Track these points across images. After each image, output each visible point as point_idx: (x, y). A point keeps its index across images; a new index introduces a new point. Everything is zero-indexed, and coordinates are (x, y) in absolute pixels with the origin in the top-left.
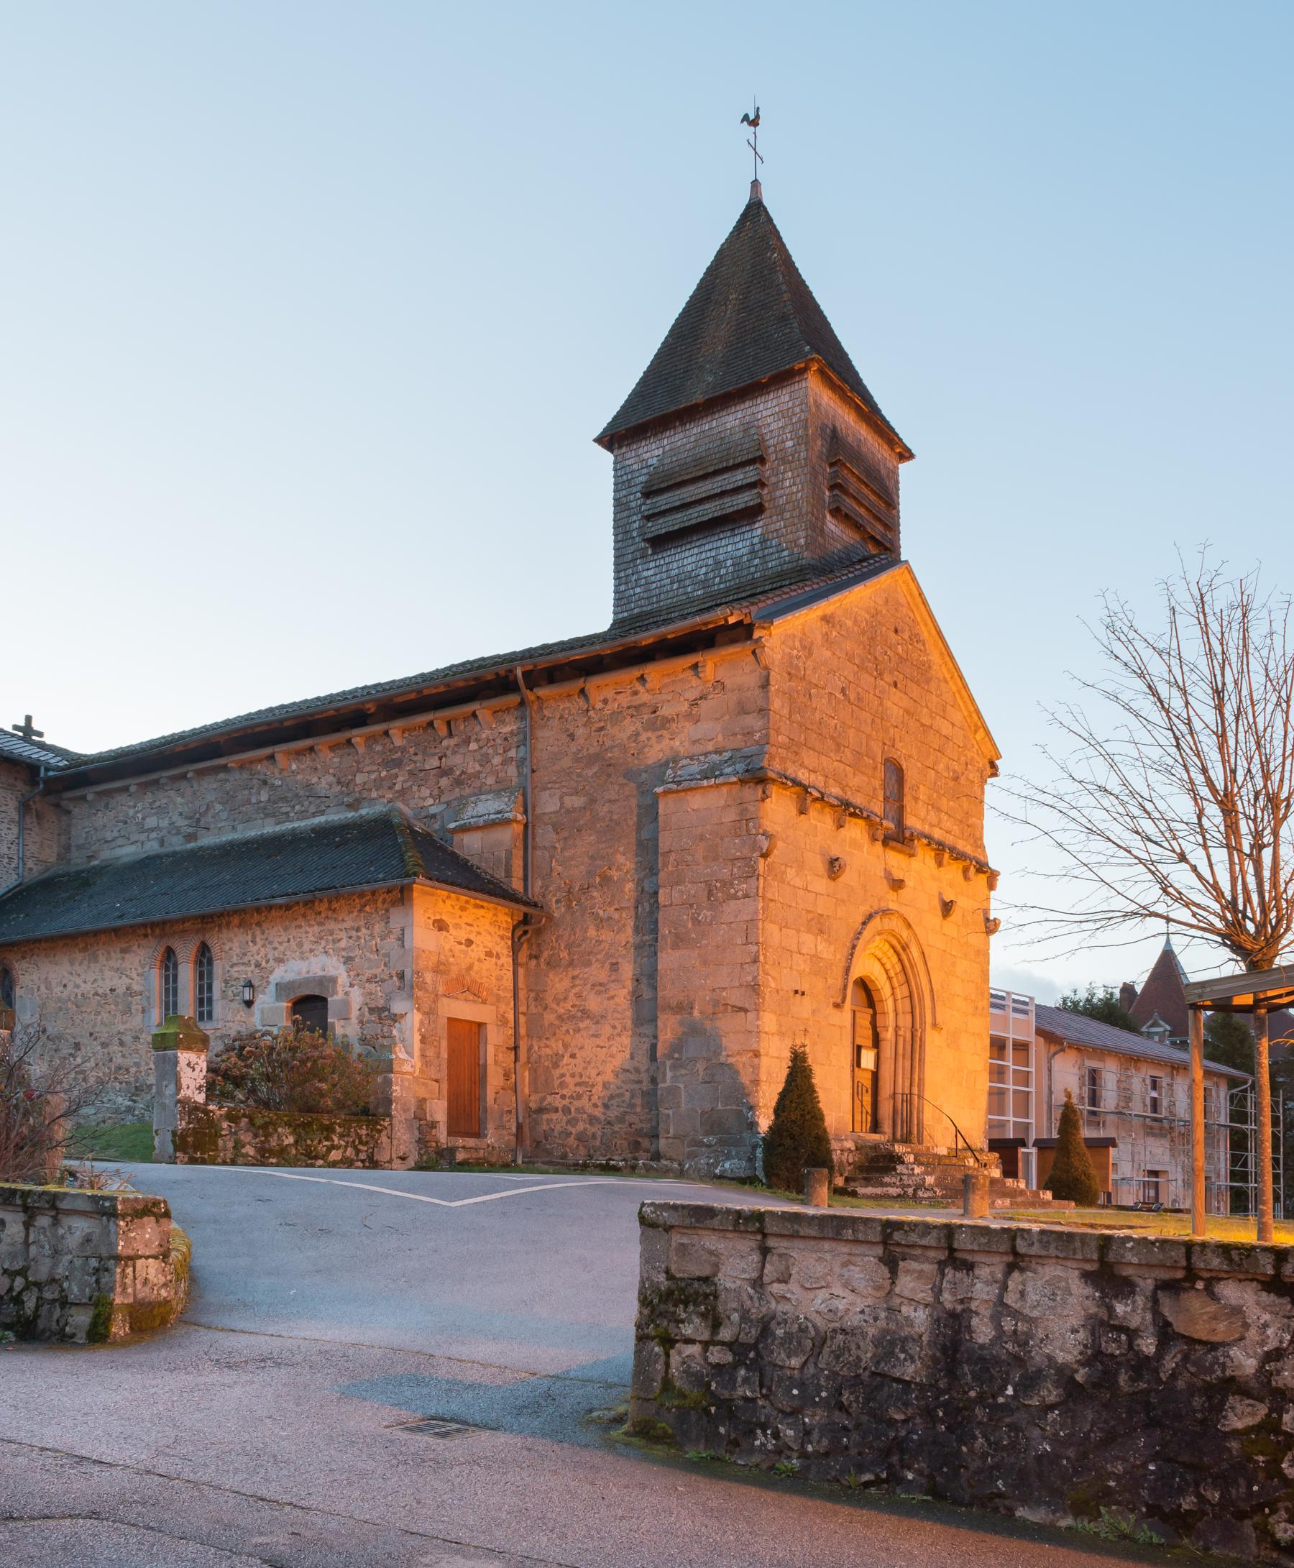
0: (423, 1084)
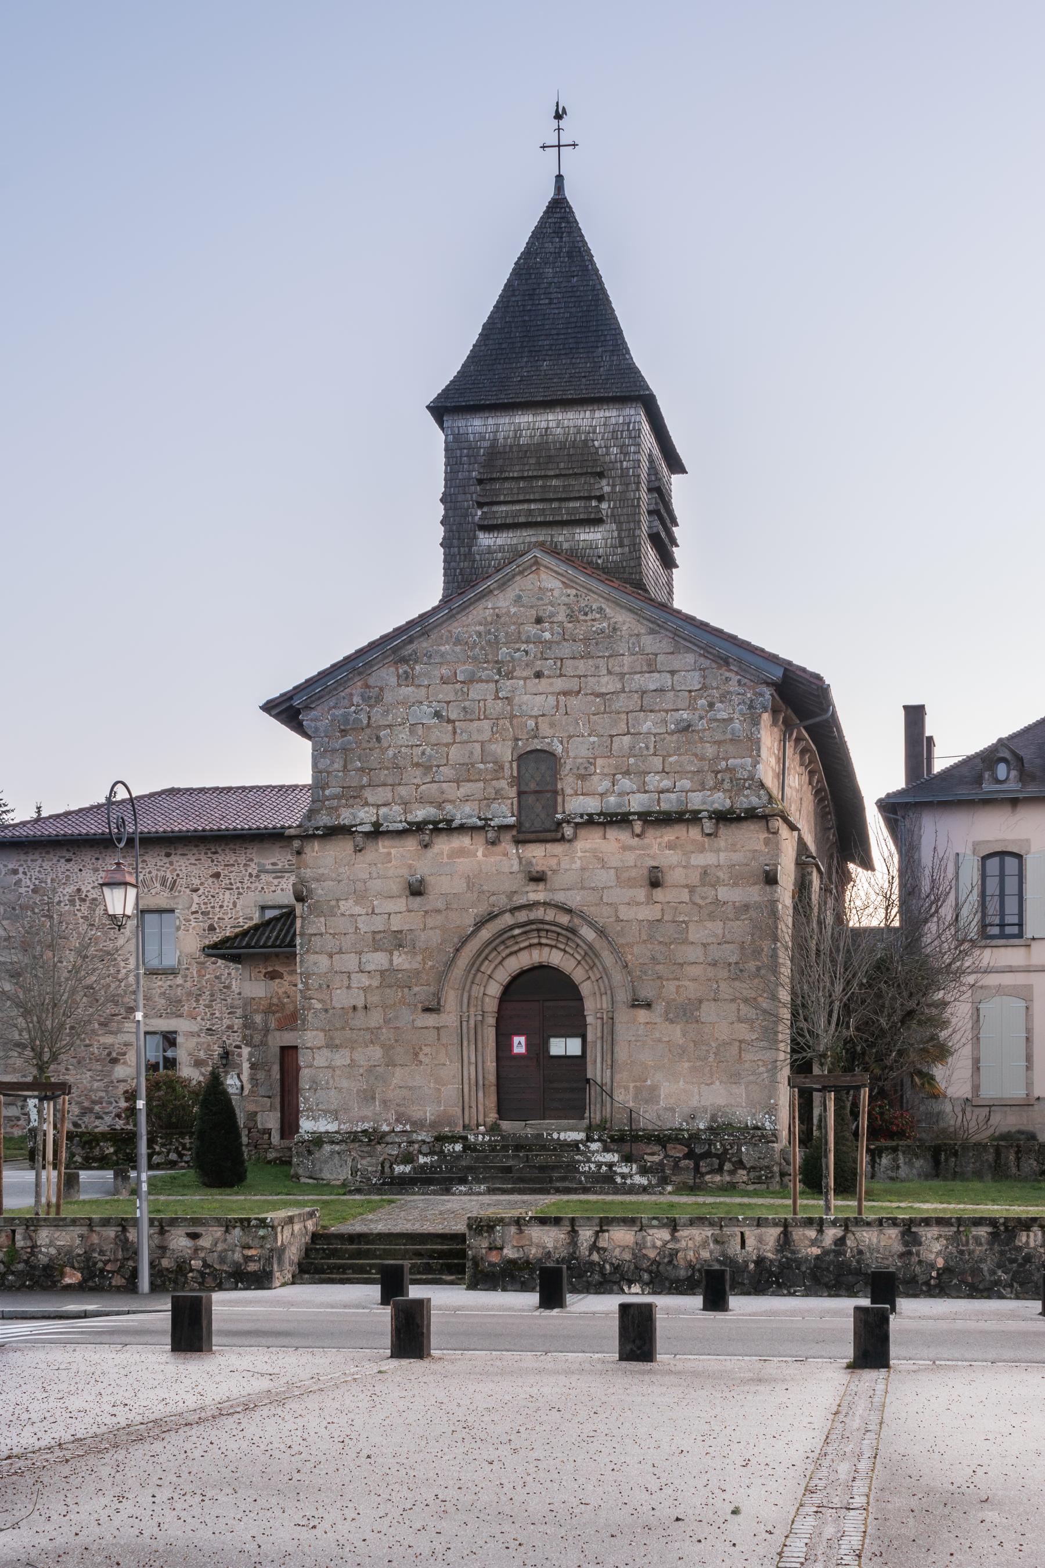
0: (253, 1101)
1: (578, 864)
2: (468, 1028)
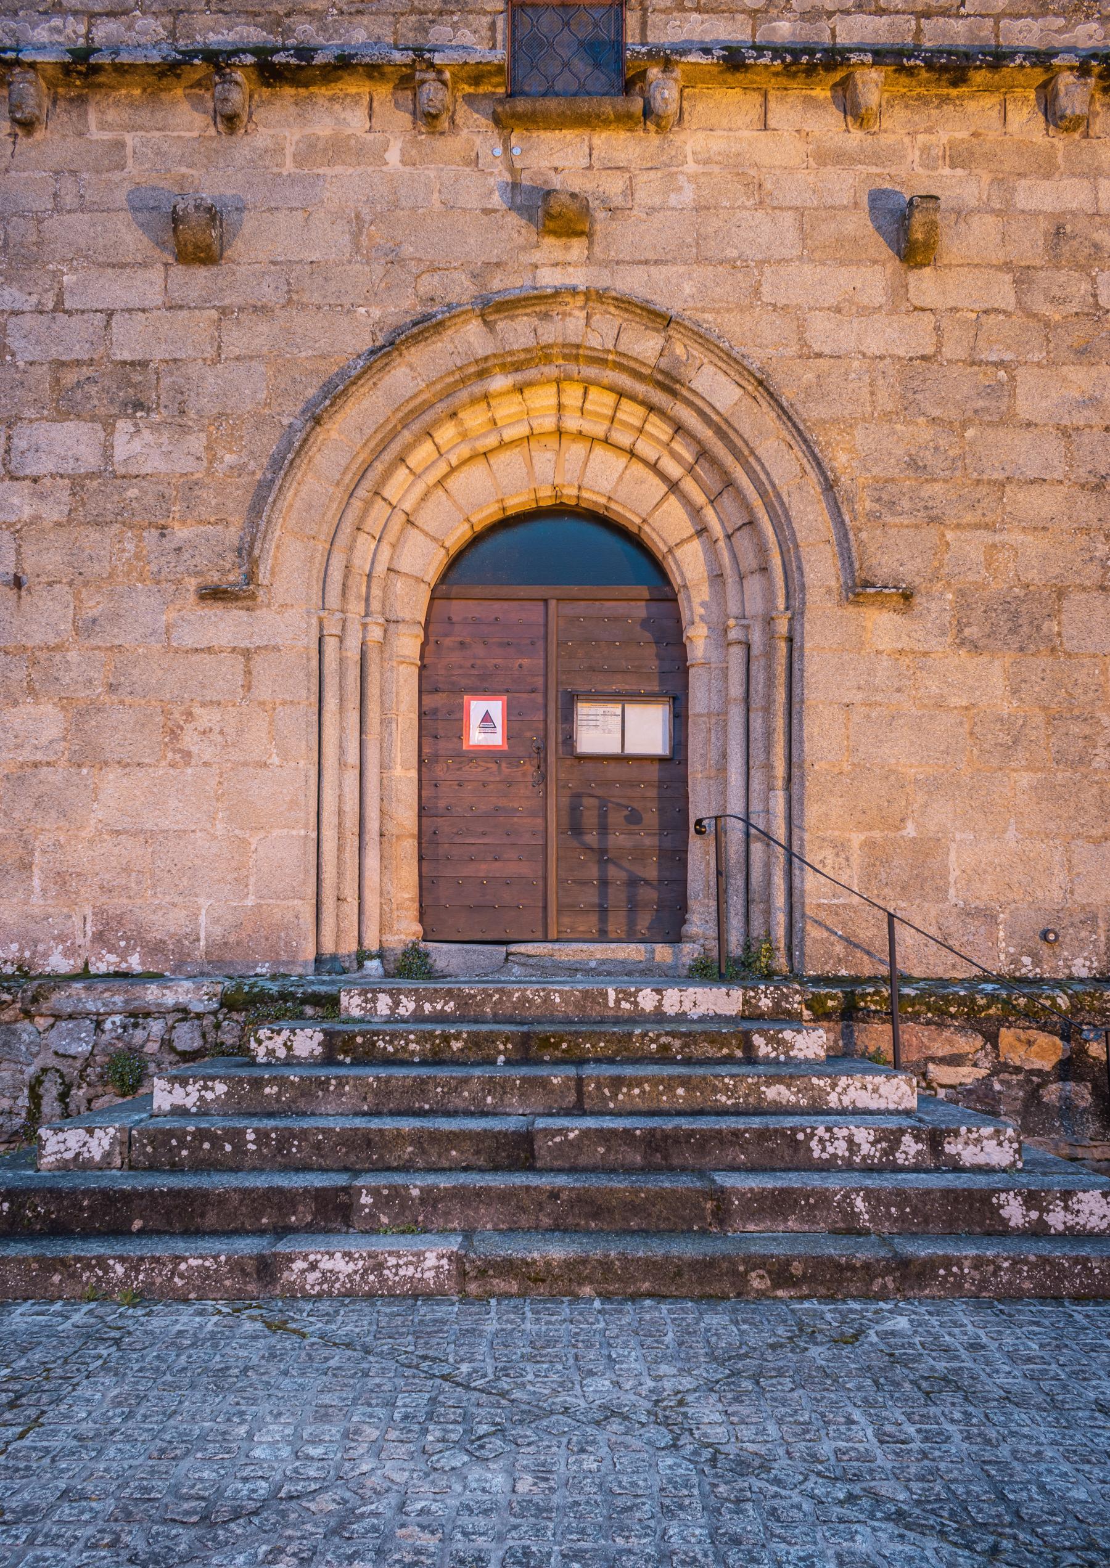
1: (687, 196)
2: (342, 661)
